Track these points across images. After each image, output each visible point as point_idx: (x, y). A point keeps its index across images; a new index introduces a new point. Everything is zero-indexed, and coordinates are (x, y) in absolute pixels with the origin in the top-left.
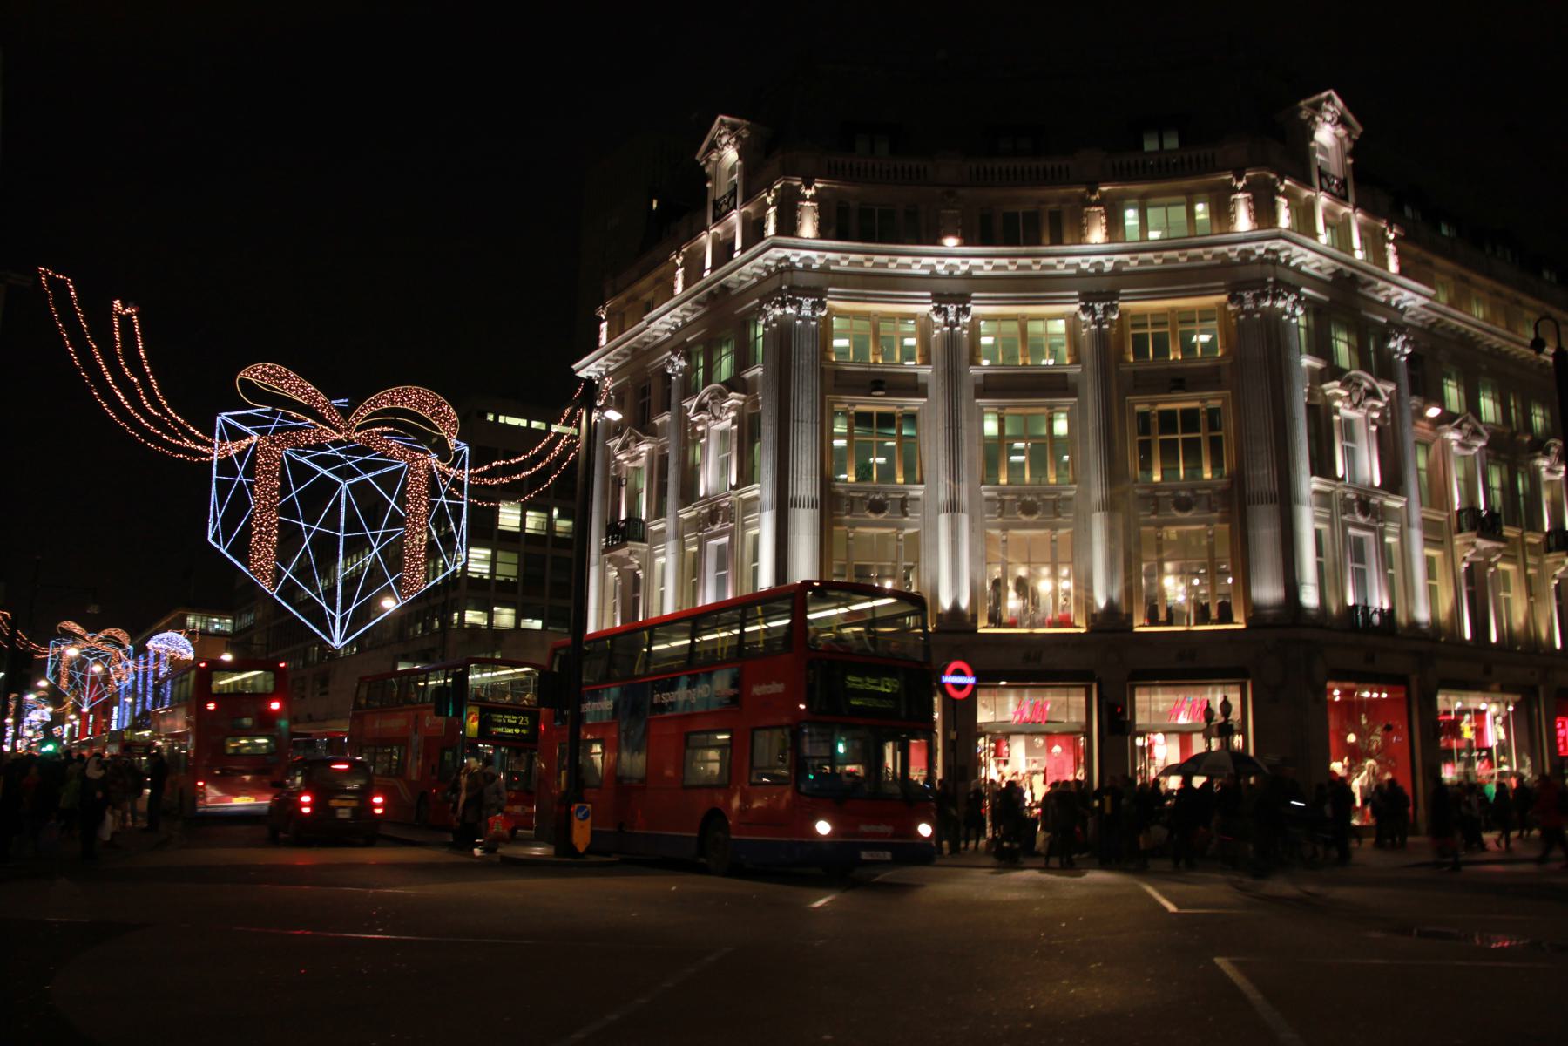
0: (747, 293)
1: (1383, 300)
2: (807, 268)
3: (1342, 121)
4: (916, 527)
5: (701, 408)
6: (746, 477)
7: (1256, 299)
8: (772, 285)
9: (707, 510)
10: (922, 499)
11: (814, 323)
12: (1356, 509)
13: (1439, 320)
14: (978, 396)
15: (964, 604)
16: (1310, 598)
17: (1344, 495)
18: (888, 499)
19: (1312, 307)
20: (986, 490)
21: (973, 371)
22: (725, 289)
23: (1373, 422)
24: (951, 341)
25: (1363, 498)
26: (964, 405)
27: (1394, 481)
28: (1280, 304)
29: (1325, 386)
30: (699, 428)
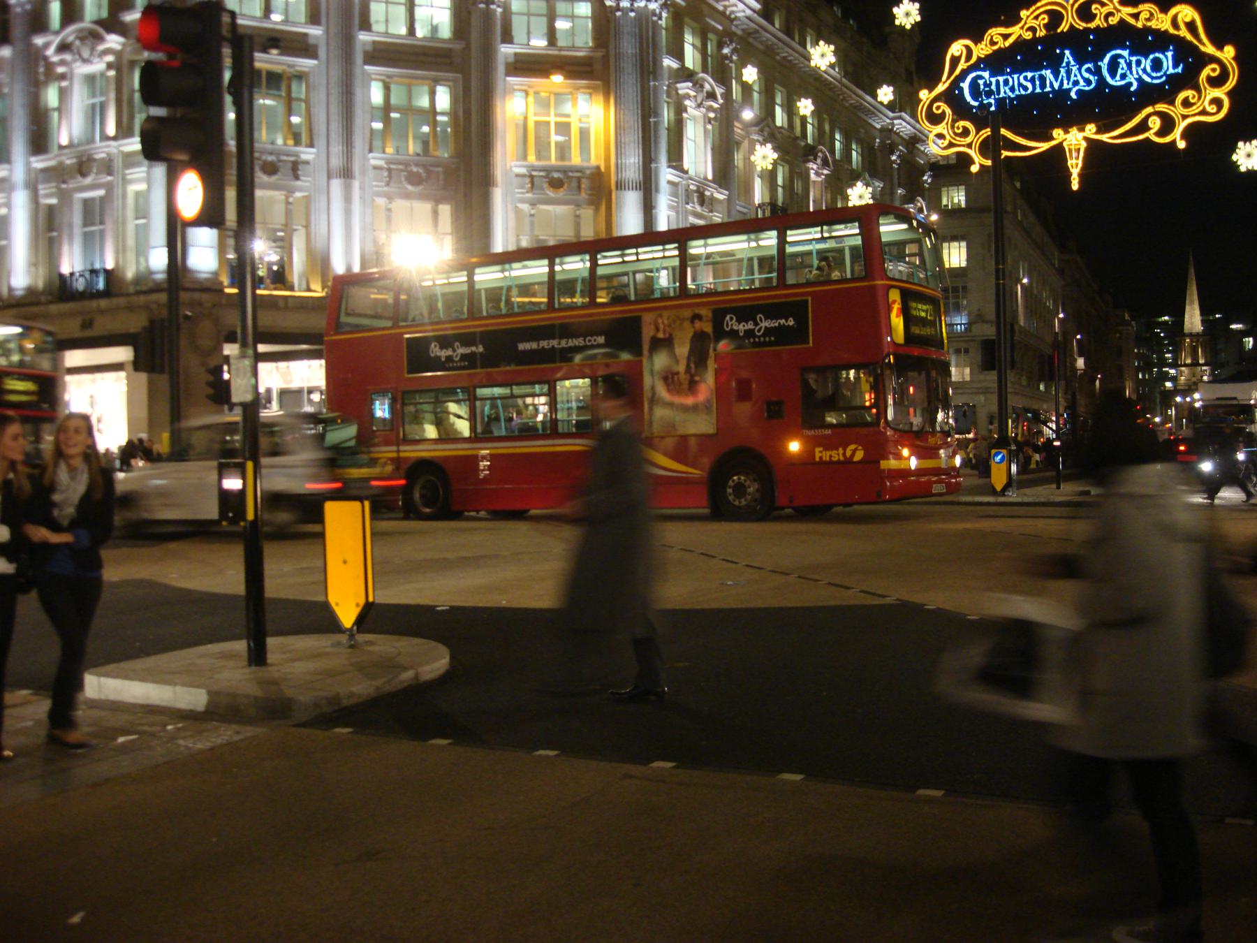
1: (721, 8)
4: (305, 191)
5: (64, 47)
9: (74, 161)
10: (312, 163)
11: (632, 14)
12: (696, 200)
13: (756, 32)
14: (508, 74)
17: (689, 186)
18: (280, 161)
20: (374, 158)
23: (710, 121)
25: (702, 190)
29: (679, 85)
30: (60, 70)
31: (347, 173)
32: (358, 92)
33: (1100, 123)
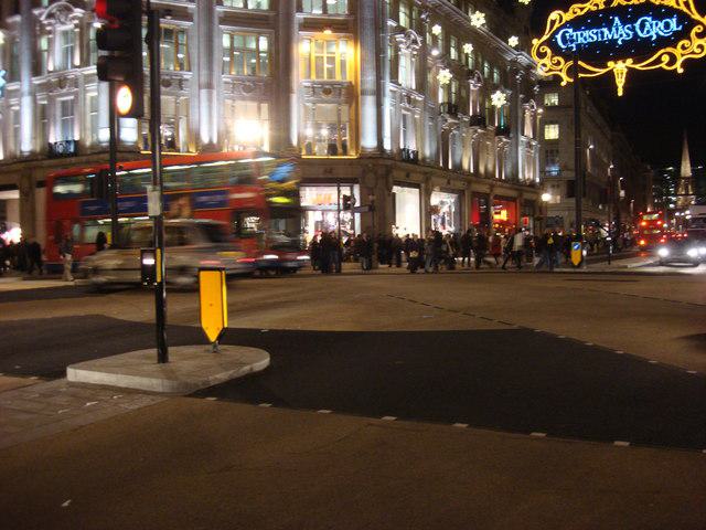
5: (50, 16)
15: (215, 141)
16: (387, 146)
30: (48, 28)
31: (209, 86)
32: (216, 40)
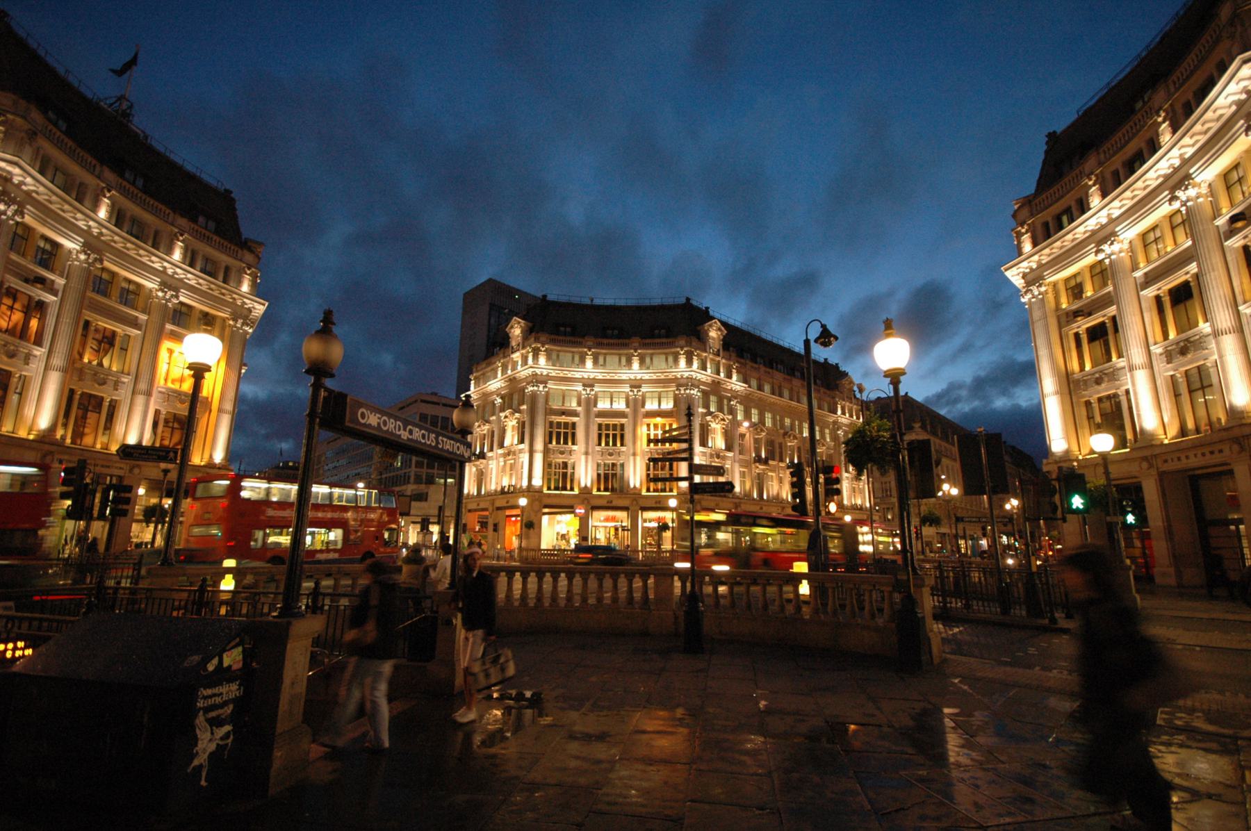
0: (522, 380)
2: (542, 374)
3: (719, 329)
5: (506, 417)
6: (522, 441)
7: (685, 390)
8: (530, 379)
19: (703, 392)
21: (595, 409)
22: (515, 378)
24: (588, 400)
26: (591, 420)
27: (729, 448)
28: (692, 392)
33: (314, 480)
